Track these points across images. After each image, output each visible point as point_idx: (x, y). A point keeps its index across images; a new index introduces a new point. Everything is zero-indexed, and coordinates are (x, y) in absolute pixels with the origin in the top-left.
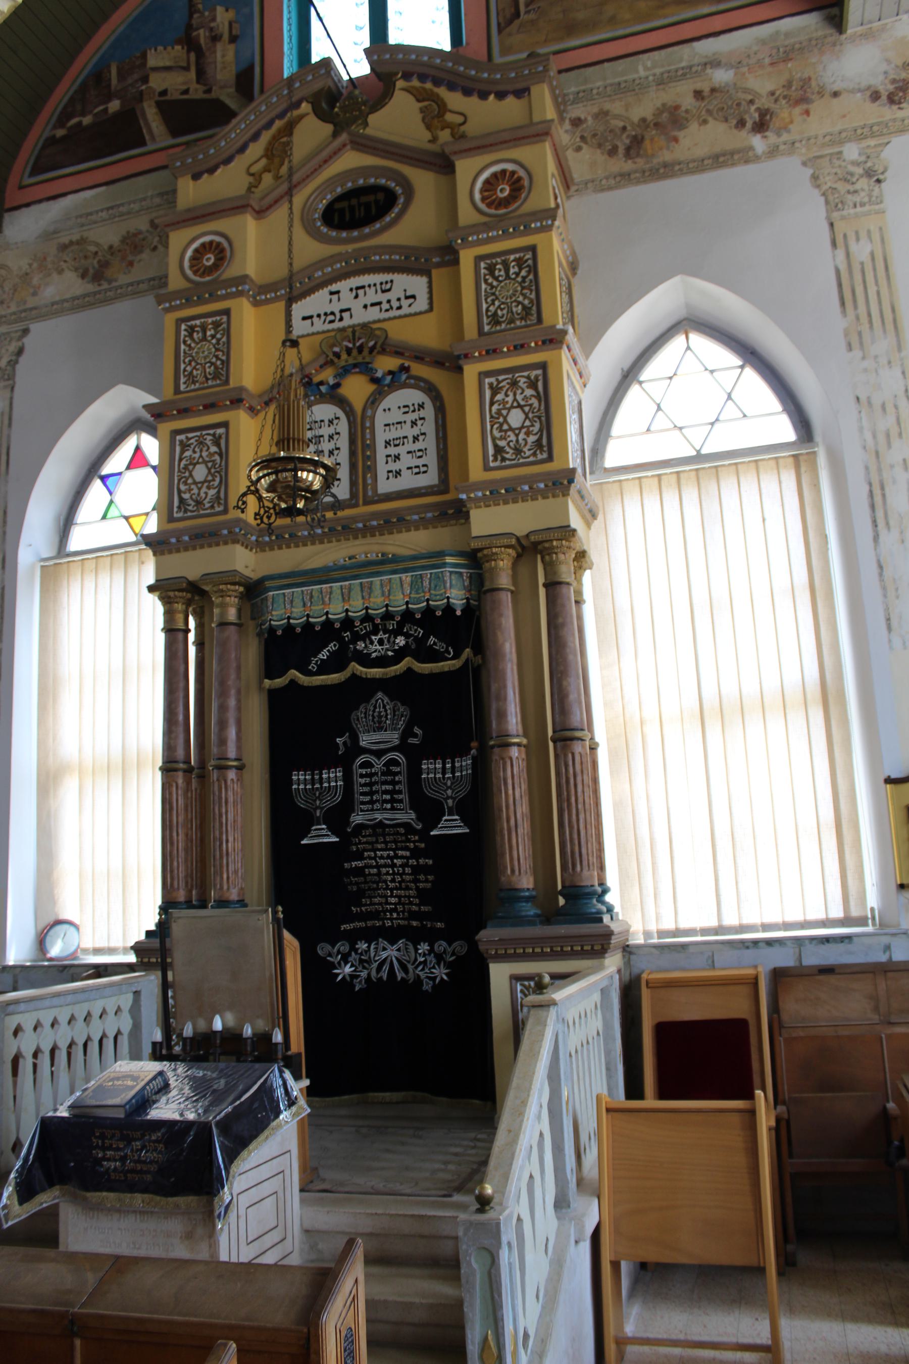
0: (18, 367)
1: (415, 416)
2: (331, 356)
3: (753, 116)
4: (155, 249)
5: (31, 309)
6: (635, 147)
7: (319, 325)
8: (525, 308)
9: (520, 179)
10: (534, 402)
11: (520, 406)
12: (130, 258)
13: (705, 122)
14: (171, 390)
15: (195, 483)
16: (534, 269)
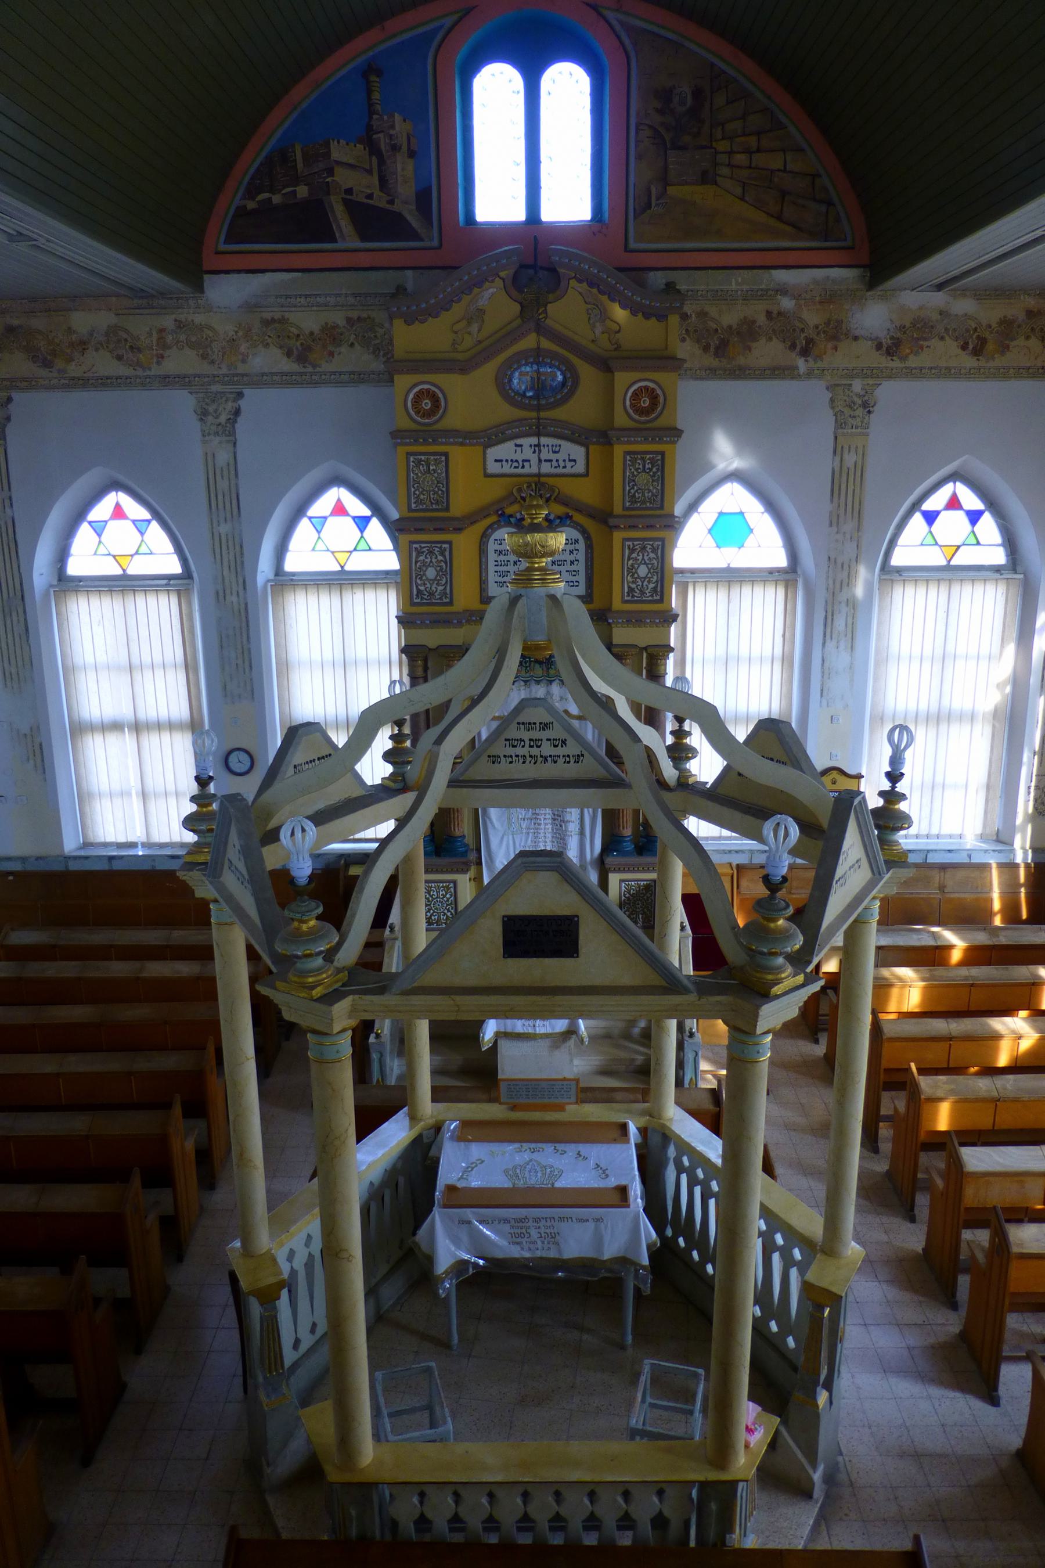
0: (237, 426)
1: (572, 547)
2: (519, 498)
3: (801, 342)
4: (352, 345)
5: (243, 375)
6: (721, 350)
7: (507, 469)
8: (653, 495)
9: (653, 390)
10: (655, 561)
11: (645, 563)
12: (330, 348)
13: (771, 339)
14: (405, 509)
15: (427, 579)
16: (662, 468)
